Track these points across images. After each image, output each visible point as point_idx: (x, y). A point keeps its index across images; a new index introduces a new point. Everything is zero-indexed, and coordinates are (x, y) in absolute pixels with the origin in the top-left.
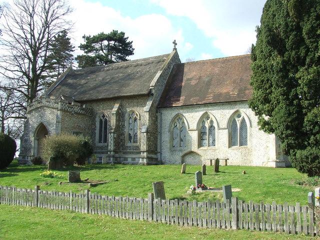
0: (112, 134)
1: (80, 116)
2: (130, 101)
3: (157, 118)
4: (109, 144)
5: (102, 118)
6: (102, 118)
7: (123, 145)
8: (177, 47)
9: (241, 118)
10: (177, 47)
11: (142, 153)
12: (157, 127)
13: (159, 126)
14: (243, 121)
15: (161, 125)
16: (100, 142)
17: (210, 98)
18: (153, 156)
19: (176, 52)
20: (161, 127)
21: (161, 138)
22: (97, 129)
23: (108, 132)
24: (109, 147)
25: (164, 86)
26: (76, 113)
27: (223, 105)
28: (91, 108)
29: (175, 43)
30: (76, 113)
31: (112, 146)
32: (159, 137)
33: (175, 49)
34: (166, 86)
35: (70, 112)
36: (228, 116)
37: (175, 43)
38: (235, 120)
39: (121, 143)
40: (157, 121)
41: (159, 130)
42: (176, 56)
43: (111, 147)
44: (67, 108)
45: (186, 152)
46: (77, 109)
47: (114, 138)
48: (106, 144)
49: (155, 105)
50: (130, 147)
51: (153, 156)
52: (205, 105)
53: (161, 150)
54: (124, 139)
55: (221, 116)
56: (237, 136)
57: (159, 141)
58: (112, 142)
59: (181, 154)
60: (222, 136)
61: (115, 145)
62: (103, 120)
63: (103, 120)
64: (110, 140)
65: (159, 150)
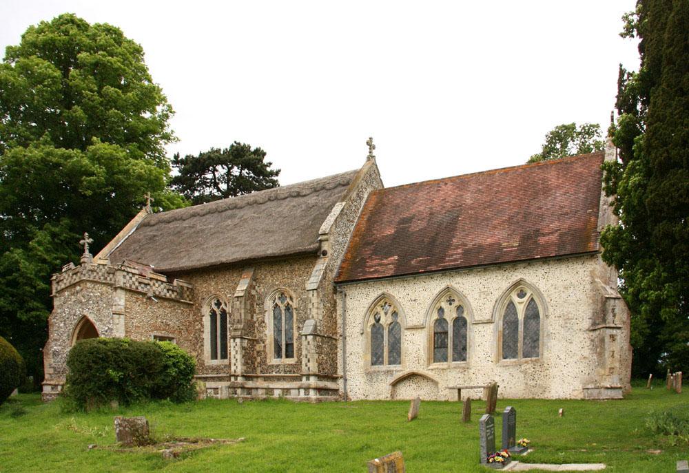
0: (238, 340)
1: (166, 303)
2: (275, 268)
3: (335, 305)
4: (233, 361)
5: (215, 308)
6: (215, 308)
7: (263, 362)
8: (375, 153)
9: (525, 299)
10: (375, 153)
11: (304, 379)
12: (336, 323)
13: (339, 321)
14: (532, 306)
15: (344, 319)
16: (214, 356)
17: (456, 256)
18: (330, 385)
19: (375, 164)
20: (344, 324)
21: (345, 346)
22: (205, 331)
23: (229, 336)
24: (233, 368)
25: (349, 236)
26: (156, 297)
27: (485, 270)
28: (190, 286)
29: (370, 144)
30: (156, 297)
31: (239, 364)
32: (340, 345)
33: (371, 157)
34: (354, 236)
35: (144, 294)
36: (497, 294)
37: (370, 144)
38: (511, 304)
39: (259, 359)
40: (335, 310)
41: (340, 331)
42: (372, 172)
43: (237, 366)
44: (137, 284)
45: (401, 374)
46: (160, 288)
47: (243, 348)
48: (226, 362)
49: (332, 275)
50: (278, 366)
51: (330, 385)
52: (446, 271)
53: (345, 371)
54: (264, 351)
55: (482, 293)
56: (522, 337)
57: (340, 353)
58: (239, 357)
59: (391, 380)
60: (484, 341)
61: (246, 363)
62: (218, 312)
63: (218, 312)
64: (233, 353)
65: (340, 372)
